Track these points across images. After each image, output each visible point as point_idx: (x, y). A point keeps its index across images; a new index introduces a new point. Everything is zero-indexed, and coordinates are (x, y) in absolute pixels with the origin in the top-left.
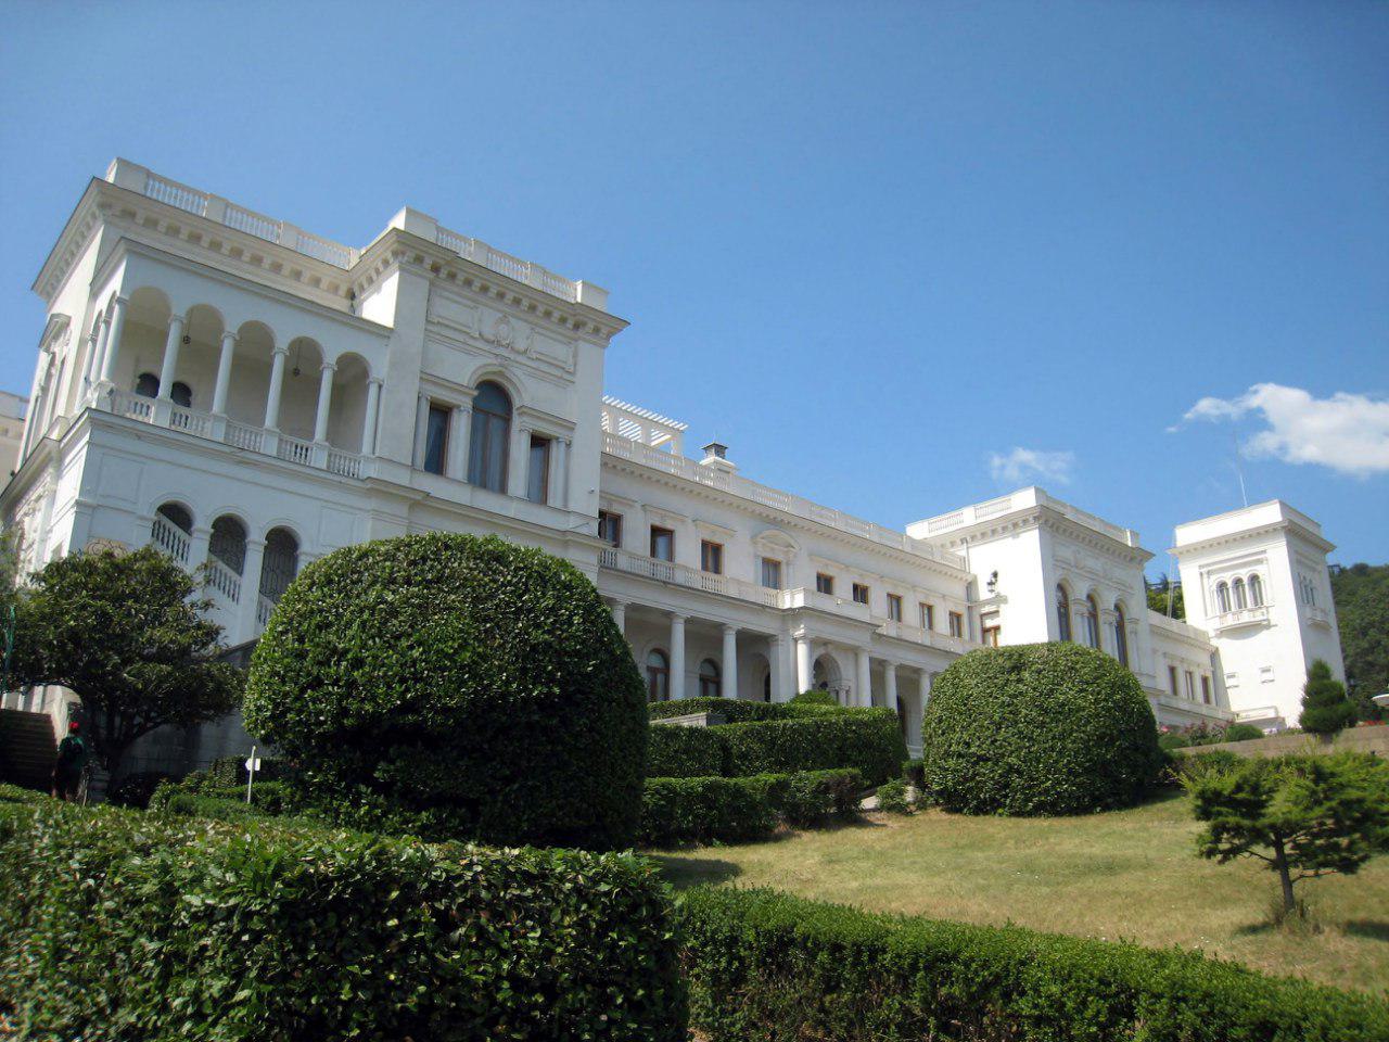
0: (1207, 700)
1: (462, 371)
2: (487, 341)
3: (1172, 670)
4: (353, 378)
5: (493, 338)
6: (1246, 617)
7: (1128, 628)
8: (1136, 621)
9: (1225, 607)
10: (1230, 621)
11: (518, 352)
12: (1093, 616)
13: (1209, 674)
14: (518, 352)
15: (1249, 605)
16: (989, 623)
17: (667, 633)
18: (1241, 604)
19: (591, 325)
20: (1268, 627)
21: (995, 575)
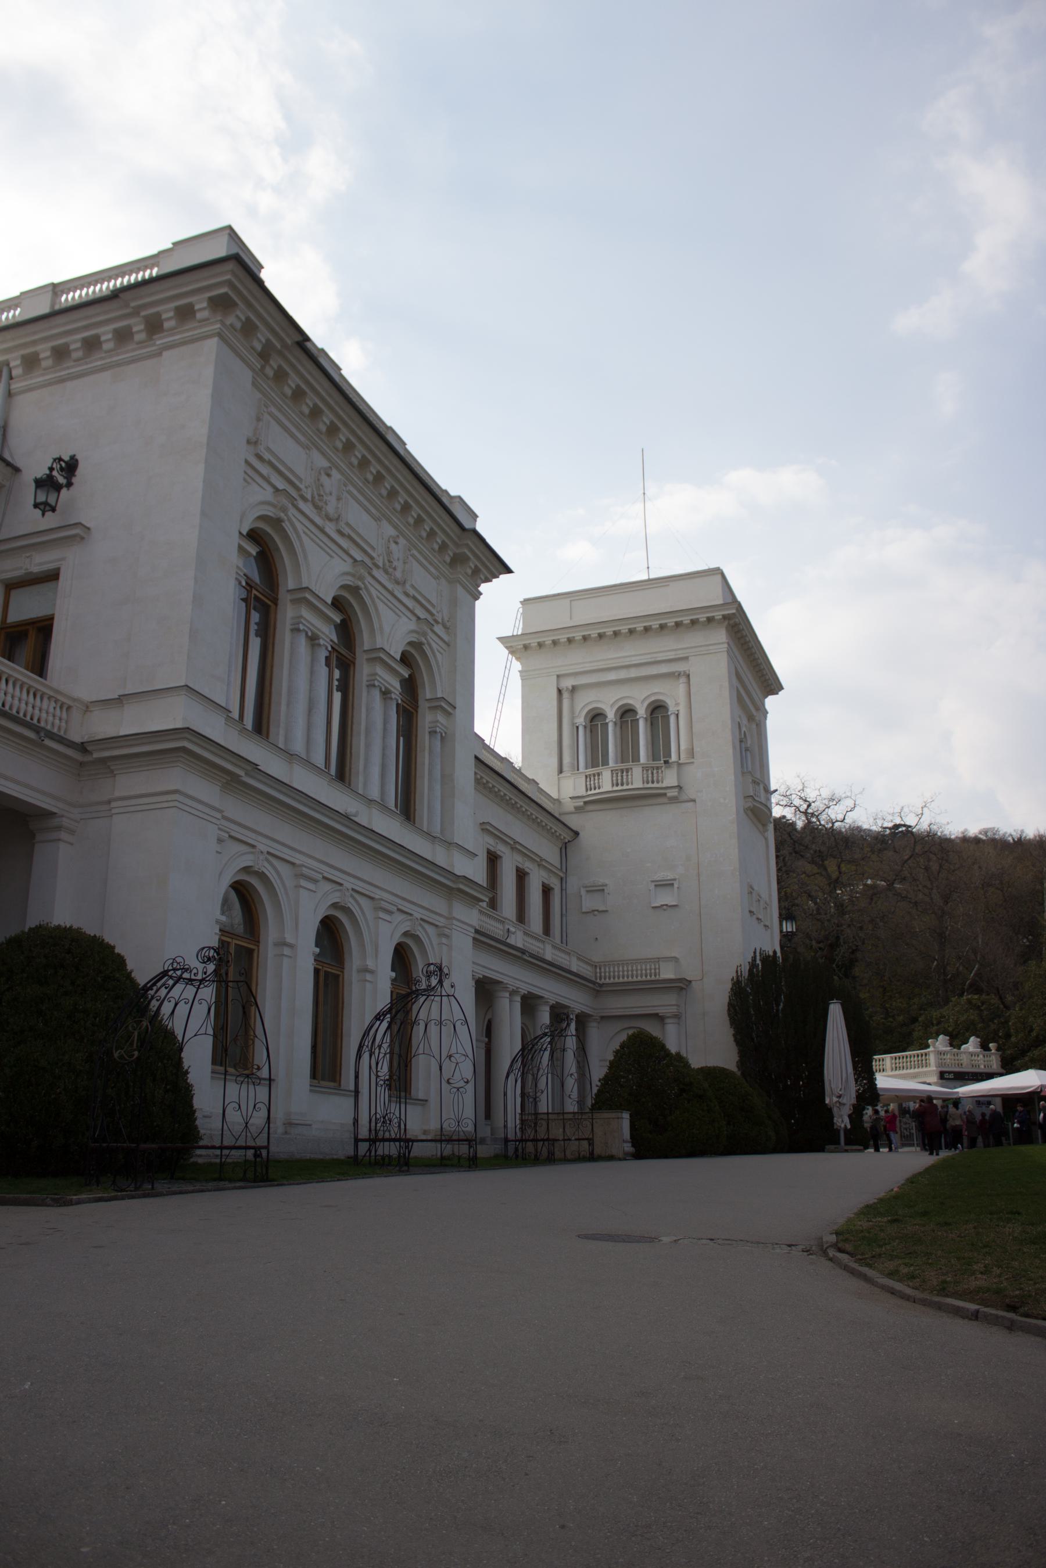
6: (637, 780)
7: (426, 719)
9: (597, 757)
10: (606, 784)
13: (555, 883)
18: (628, 752)
20: (674, 800)
21: (70, 467)
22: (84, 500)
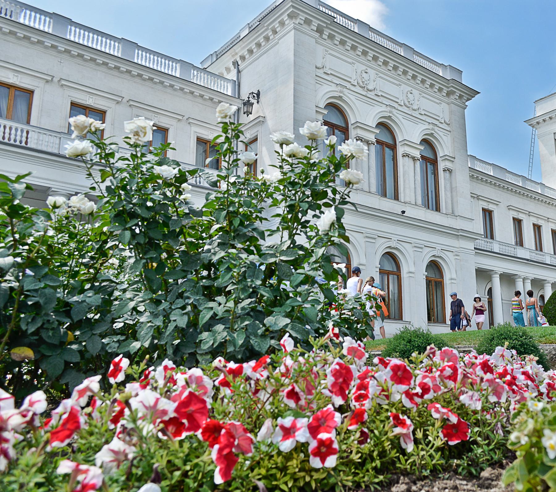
3: (518, 222)
21: (258, 94)
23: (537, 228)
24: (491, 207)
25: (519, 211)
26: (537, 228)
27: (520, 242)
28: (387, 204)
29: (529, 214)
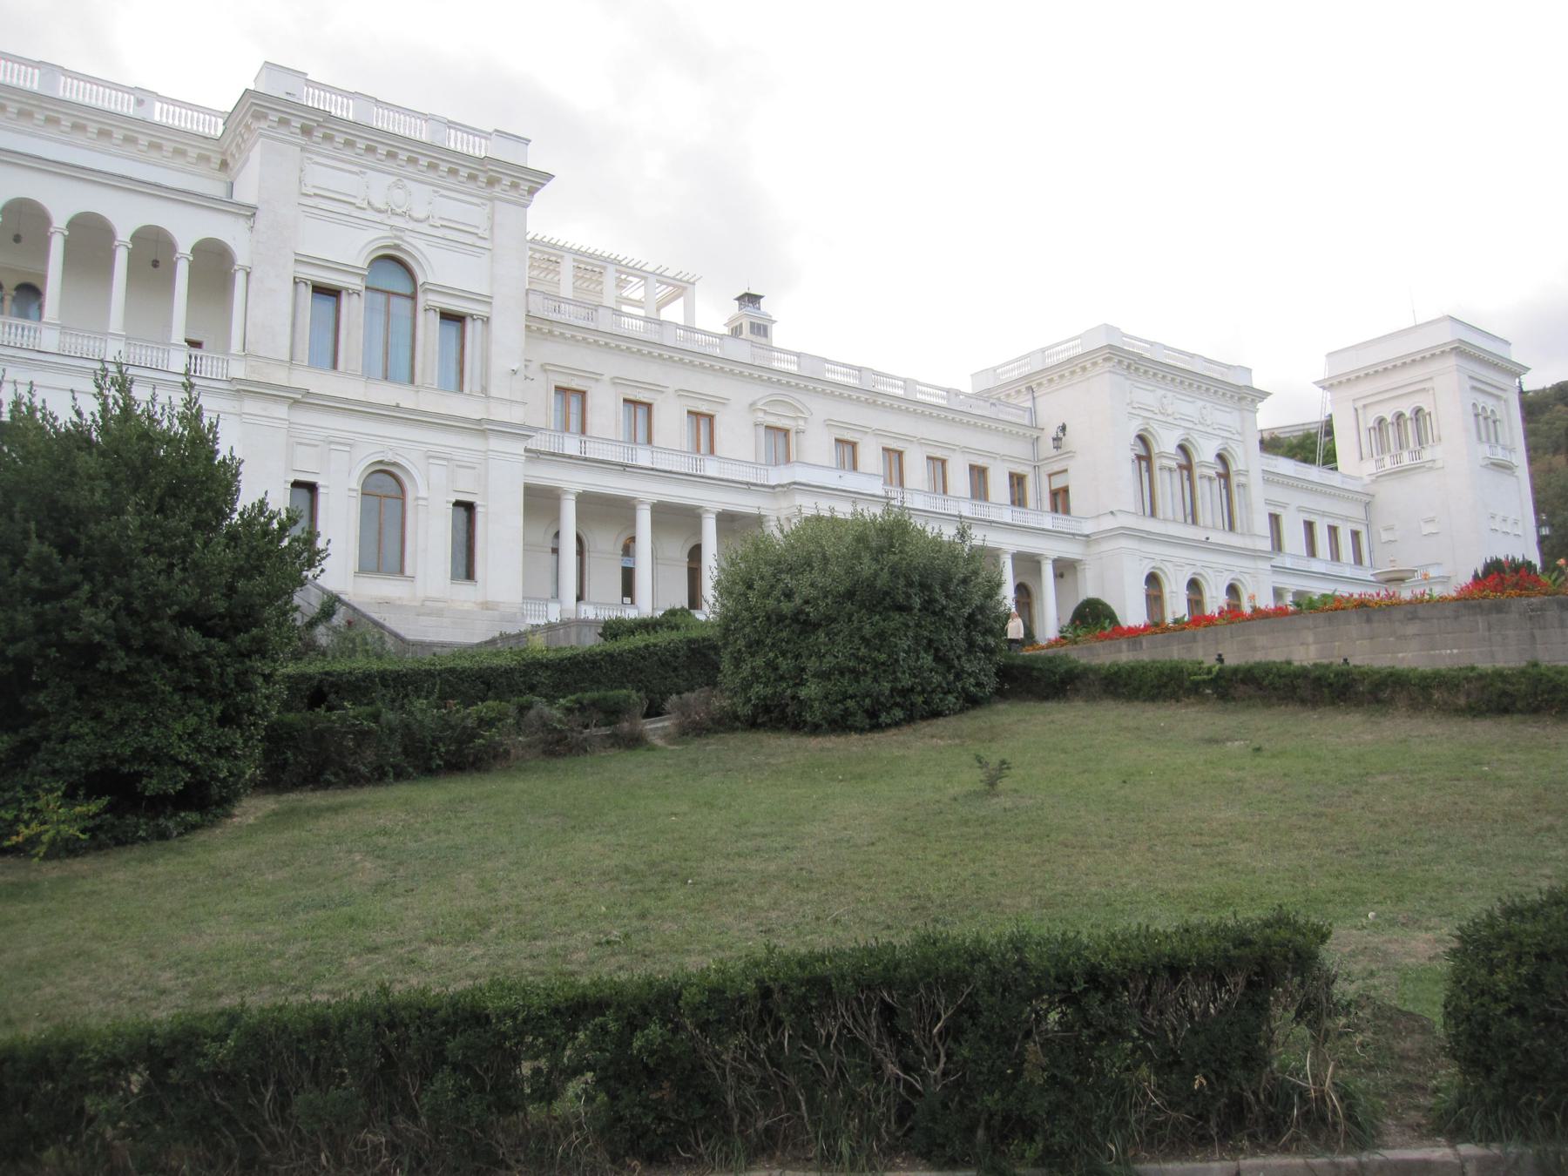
0: (1358, 559)
1: (346, 250)
2: (380, 211)
3: (1309, 526)
4: (214, 266)
5: (383, 207)
6: (1406, 459)
7: (1234, 480)
8: (1245, 473)
10: (1388, 463)
11: (417, 221)
12: (1187, 467)
14: (417, 221)
15: (1411, 445)
16: (1058, 483)
17: (631, 522)
19: (507, 181)
21: (1063, 428)
22: (1070, 440)
23: (1333, 530)
24: (1277, 511)
25: (1310, 511)
26: (1333, 530)
27: (1312, 552)
28: (1189, 532)
29: (1324, 514)
